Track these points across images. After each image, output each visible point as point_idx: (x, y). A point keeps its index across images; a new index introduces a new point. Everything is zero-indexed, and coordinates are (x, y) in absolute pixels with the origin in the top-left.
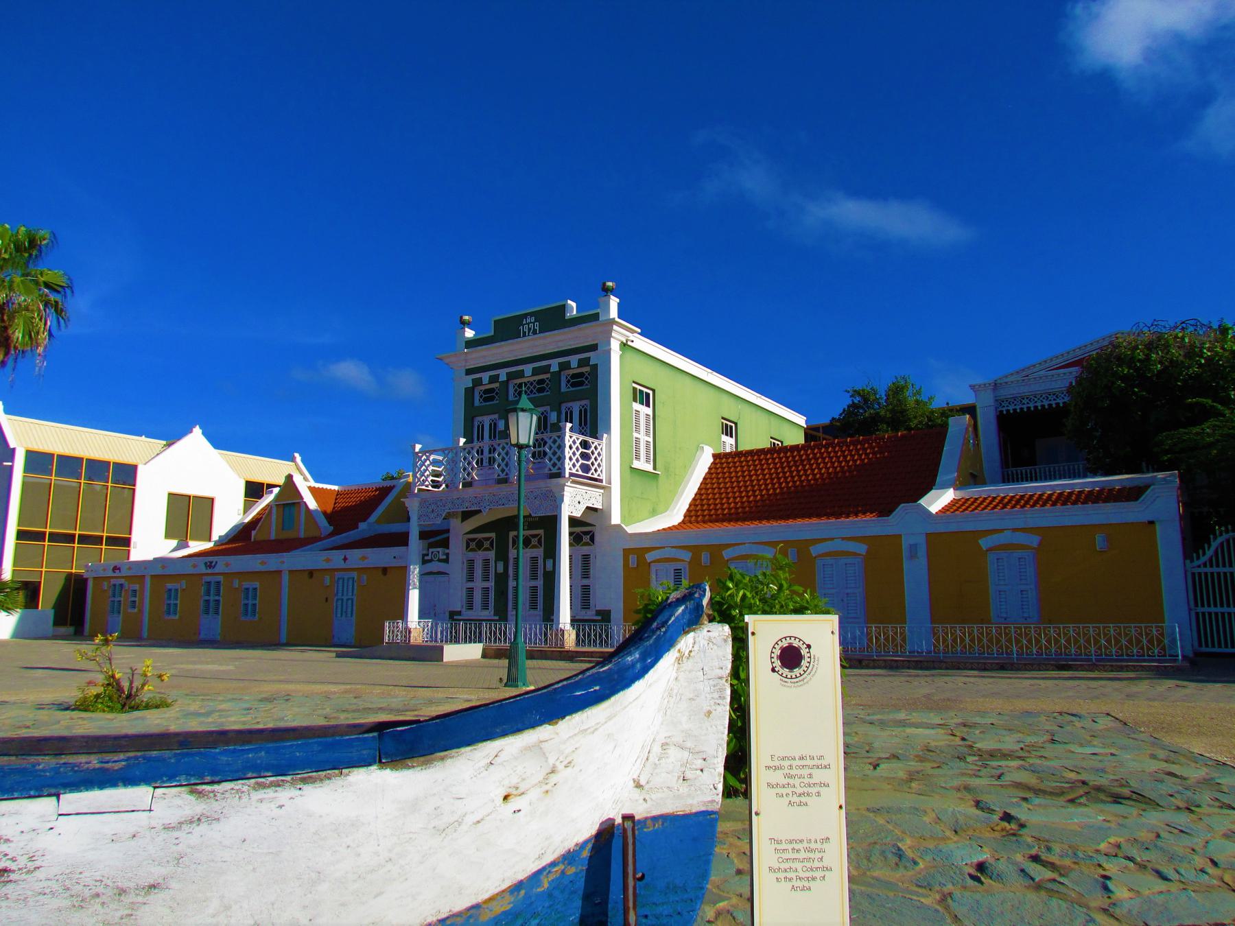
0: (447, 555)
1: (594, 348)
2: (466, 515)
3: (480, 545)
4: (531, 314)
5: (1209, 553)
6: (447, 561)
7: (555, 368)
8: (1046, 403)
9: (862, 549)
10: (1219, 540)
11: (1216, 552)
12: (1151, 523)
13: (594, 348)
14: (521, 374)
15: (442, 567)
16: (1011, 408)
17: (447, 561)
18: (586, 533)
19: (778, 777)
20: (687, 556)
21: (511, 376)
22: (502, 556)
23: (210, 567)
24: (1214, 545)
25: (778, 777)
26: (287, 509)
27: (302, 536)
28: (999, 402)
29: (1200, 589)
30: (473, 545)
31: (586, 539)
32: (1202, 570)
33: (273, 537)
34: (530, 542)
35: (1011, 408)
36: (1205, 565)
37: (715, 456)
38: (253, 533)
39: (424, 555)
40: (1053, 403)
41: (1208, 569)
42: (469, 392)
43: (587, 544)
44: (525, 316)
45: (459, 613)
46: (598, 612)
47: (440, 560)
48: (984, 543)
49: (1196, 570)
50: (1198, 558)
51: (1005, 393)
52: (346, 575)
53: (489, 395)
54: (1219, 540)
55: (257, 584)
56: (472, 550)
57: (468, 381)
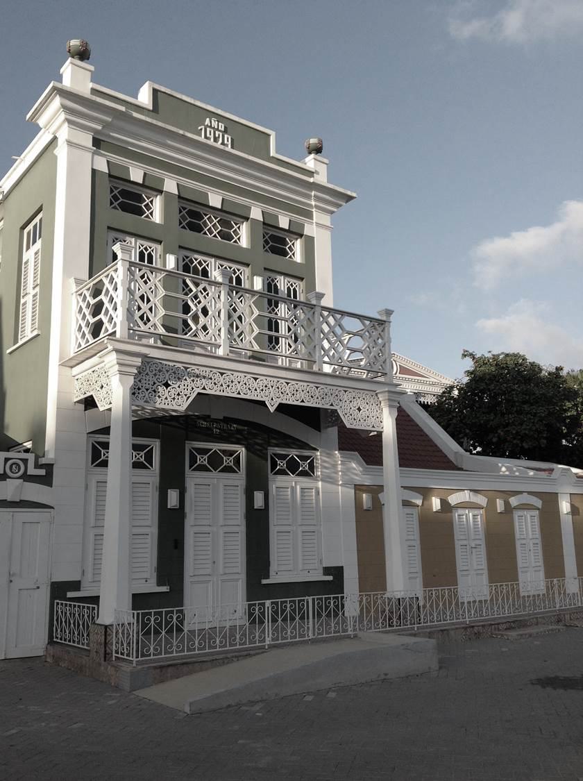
4: (220, 118)
7: (256, 213)
15: (34, 492)
18: (304, 458)
31: (304, 466)
43: (304, 474)
45: (76, 585)
46: (327, 571)
47: (27, 478)
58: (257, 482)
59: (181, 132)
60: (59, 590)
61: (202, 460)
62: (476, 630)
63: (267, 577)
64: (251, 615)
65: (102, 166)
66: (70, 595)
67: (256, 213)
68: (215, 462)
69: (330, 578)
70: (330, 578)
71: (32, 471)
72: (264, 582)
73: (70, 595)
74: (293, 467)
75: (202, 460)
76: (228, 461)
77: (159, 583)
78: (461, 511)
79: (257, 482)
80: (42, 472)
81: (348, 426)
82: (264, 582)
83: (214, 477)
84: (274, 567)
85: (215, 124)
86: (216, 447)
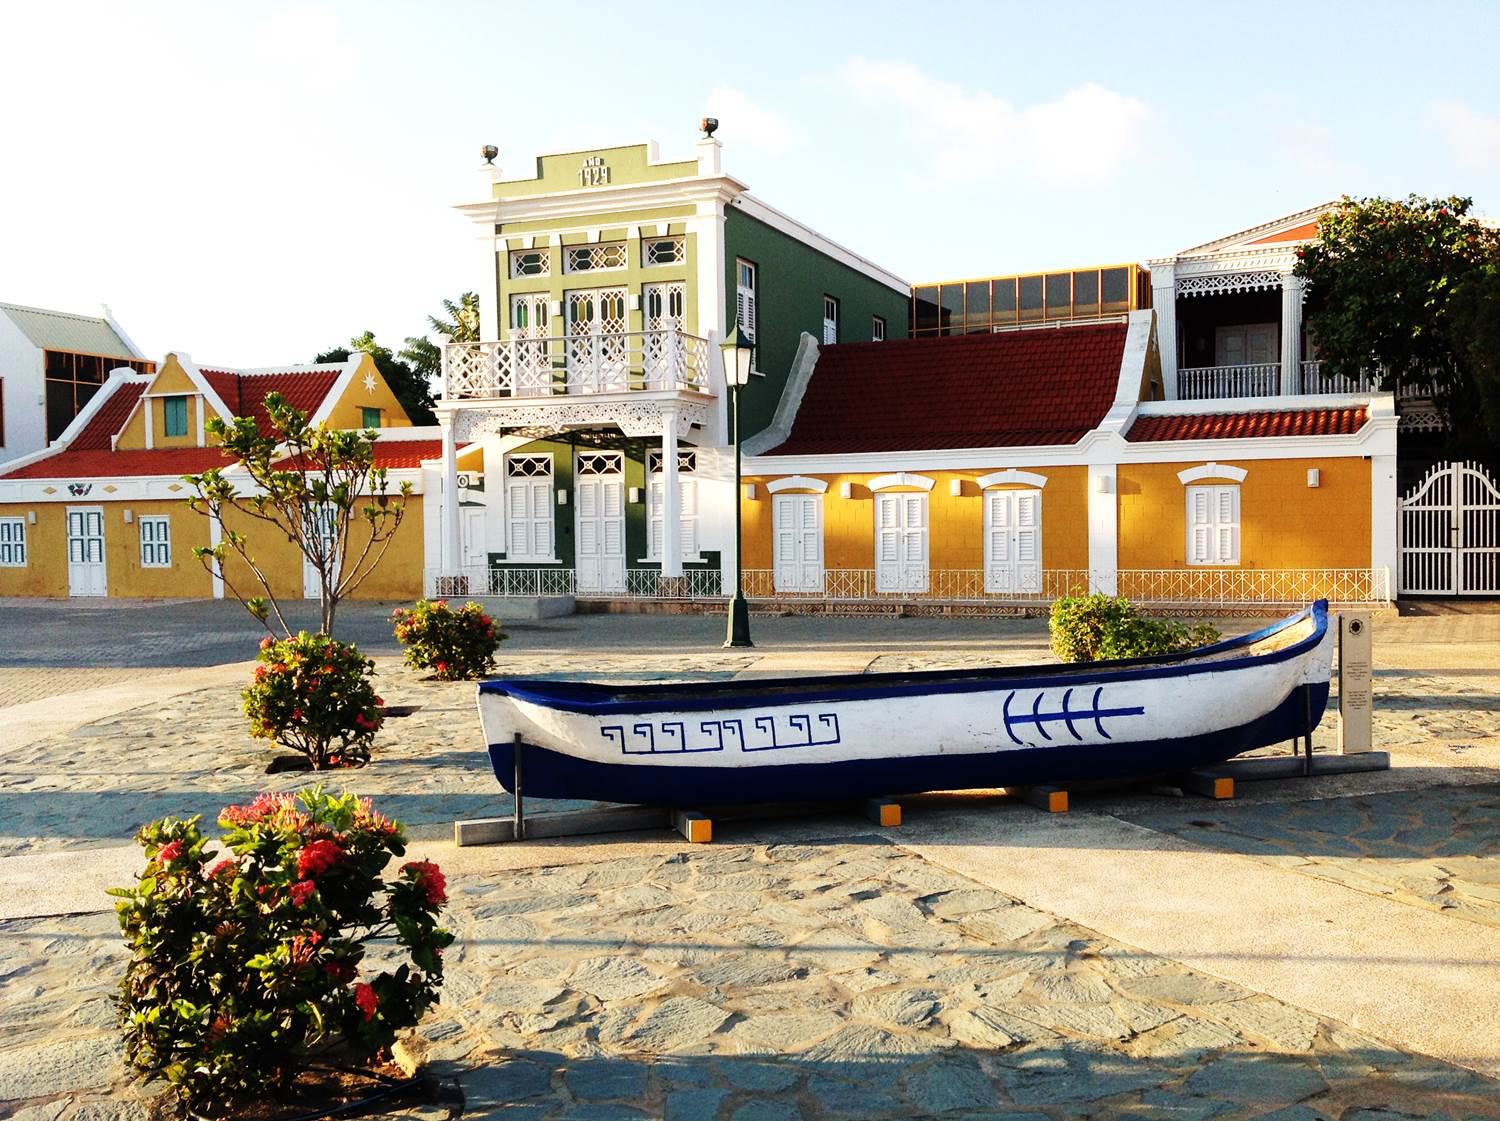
0: (481, 480)
1: (690, 209)
2: (505, 431)
3: (529, 468)
5: (1424, 490)
6: (481, 487)
8: (1238, 287)
9: (1041, 481)
10: (1441, 473)
11: (1430, 489)
12: (1368, 458)
15: (474, 496)
16: (1194, 291)
17: (481, 487)
19: (1350, 670)
23: (80, 492)
24: (1430, 481)
25: (1350, 670)
26: (171, 406)
27: (201, 443)
28: (1181, 282)
29: (1412, 528)
30: (519, 467)
32: (1415, 508)
33: (149, 445)
34: (604, 464)
35: (1194, 291)
36: (1417, 503)
37: (821, 347)
38: (114, 438)
40: (1247, 286)
41: (1421, 508)
45: (503, 556)
46: (703, 555)
47: (469, 487)
48: (1185, 476)
49: (1406, 509)
50: (1411, 496)
51: (1188, 271)
53: (530, 262)
54: (1441, 473)
56: (519, 474)
59: (544, 196)
60: (492, 557)
61: (588, 465)
62: (695, 606)
64: (630, 584)
65: (502, 248)
66: (498, 561)
68: (599, 465)
69: (705, 561)
70: (705, 561)
72: (640, 561)
73: (498, 561)
75: (588, 465)
76: (611, 464)
77: (557, 558)
78: (888, 497)
81: (628, 435)
82: (640, 561)
84: (650, 552)
86: (599, 454)
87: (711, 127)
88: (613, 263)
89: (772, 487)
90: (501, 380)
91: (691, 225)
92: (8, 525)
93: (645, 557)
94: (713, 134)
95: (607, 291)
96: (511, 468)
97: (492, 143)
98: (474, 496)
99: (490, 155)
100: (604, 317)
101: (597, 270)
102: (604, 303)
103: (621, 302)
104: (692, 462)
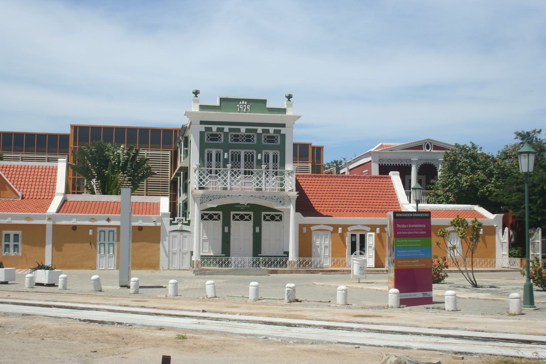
3: (211, 217)
4: (245, 100)
13: (283, 126)
14: (239, 130)
15: (185, 228)
17: (188, 224)
20: (331, 229)
21: (230, 130)
22: (226, 223)
30: (206, 217)
31: (277, 218)
39: (171, 221)
42: (202, 133)
44: (241, 100)
47: (183, 224)
52: (107, 229)
53: (214, 137)
55: (19, 232)
57: (202, 128)
58: (257, 223)
63: (260, 253)
67: (260, 130)
68: (242, 218)
71: (184, 222)
74: (273, 218)
76: (247, 217)
77: (222, 253)
79: (257, 223)
80: (187, 222)
83: (242, 222)
85: (243, 103)
87: (289, 97)
88: (250, 141)
89: (312, 228)
90: (257, 184)
91: (283, 131)
92: (113, 231)
93: (260, 253)
94: (290, 99)
95: (247, 151)
96: (202, 217)
97: (194, 89)
98: (185, 228)
99: (196, 93)
100: (245, 160)
101: (242, 143)
102: (245, 156)
103: (253, 156)
104: (281, 218)
